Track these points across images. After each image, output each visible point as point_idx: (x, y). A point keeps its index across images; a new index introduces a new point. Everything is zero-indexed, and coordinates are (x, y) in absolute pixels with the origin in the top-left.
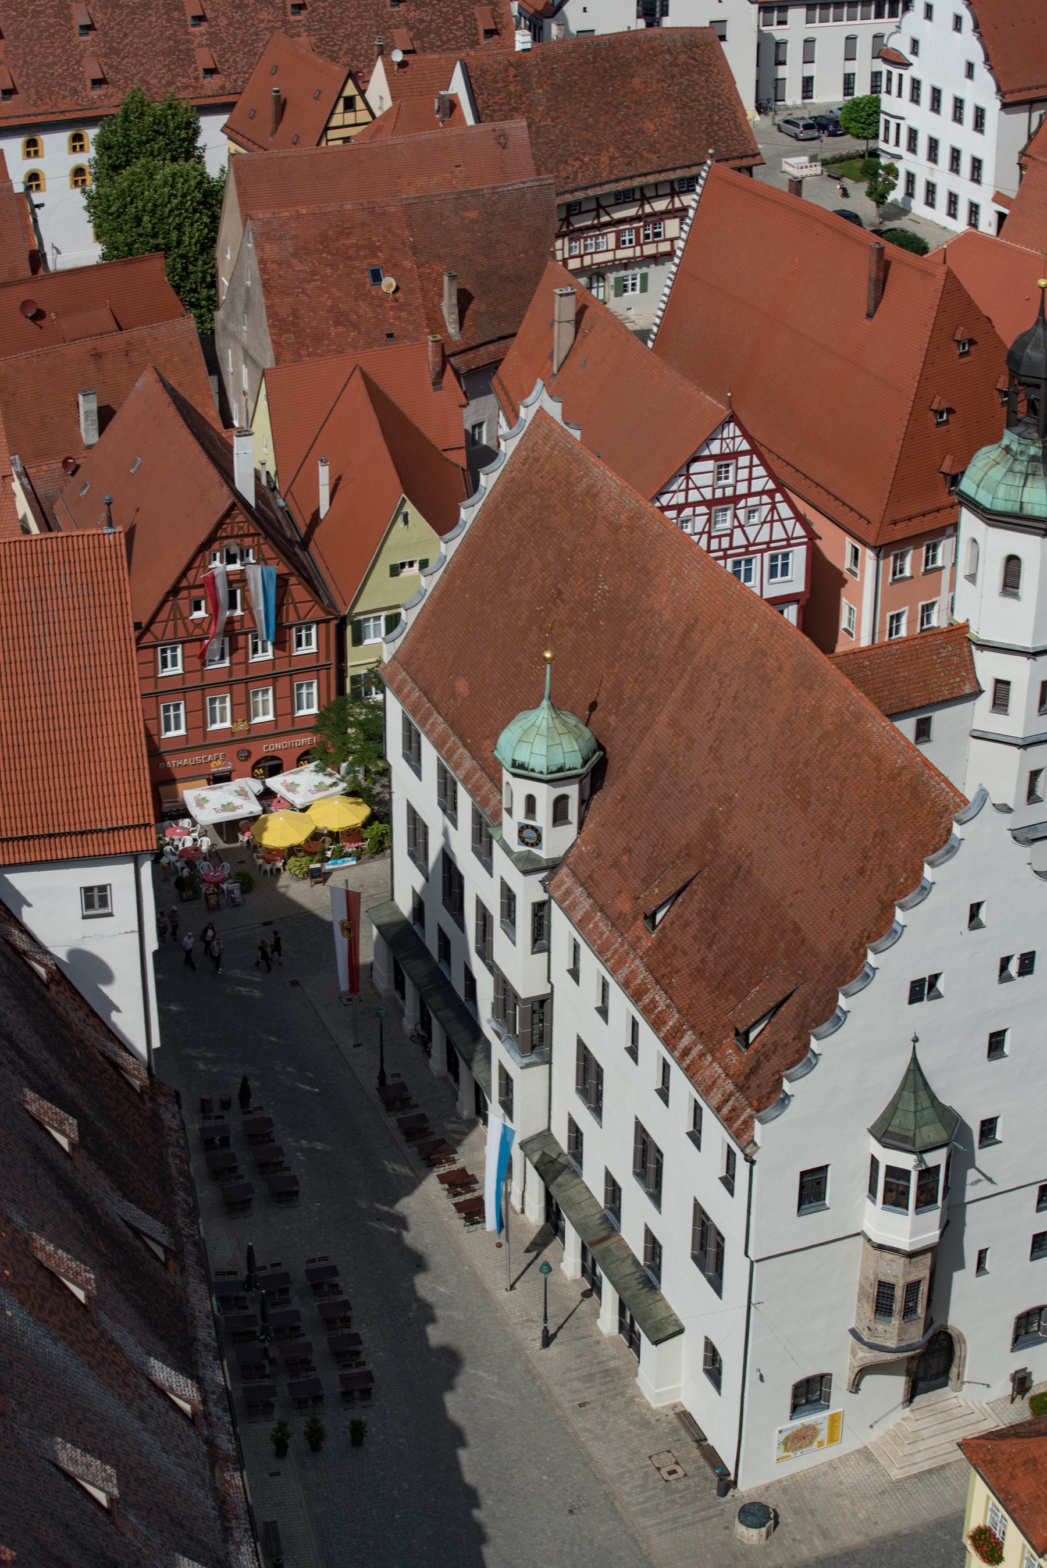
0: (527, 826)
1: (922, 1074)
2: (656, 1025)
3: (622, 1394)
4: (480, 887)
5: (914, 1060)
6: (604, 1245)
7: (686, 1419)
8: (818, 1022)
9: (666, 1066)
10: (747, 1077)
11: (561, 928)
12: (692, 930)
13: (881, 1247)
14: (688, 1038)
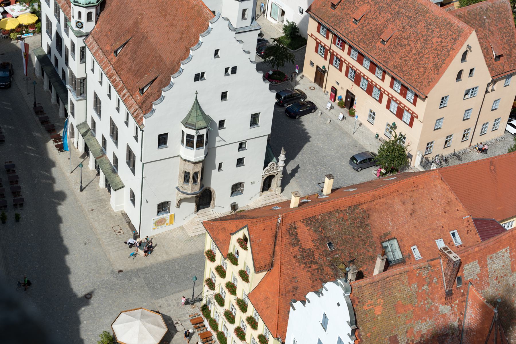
0: (79, 22)
1: (199, 104)
2: (115, 87)
3: (105, 207)
4: (67, 43)
5: (196, 100)
6: (101, 159)
7: (125, 215)
8: (165, 86)
9: (119, 100)
10: (142, 104)
11: (89, 55)
12: (128, 56)
13: (185, 160)
14: (125, 91)
